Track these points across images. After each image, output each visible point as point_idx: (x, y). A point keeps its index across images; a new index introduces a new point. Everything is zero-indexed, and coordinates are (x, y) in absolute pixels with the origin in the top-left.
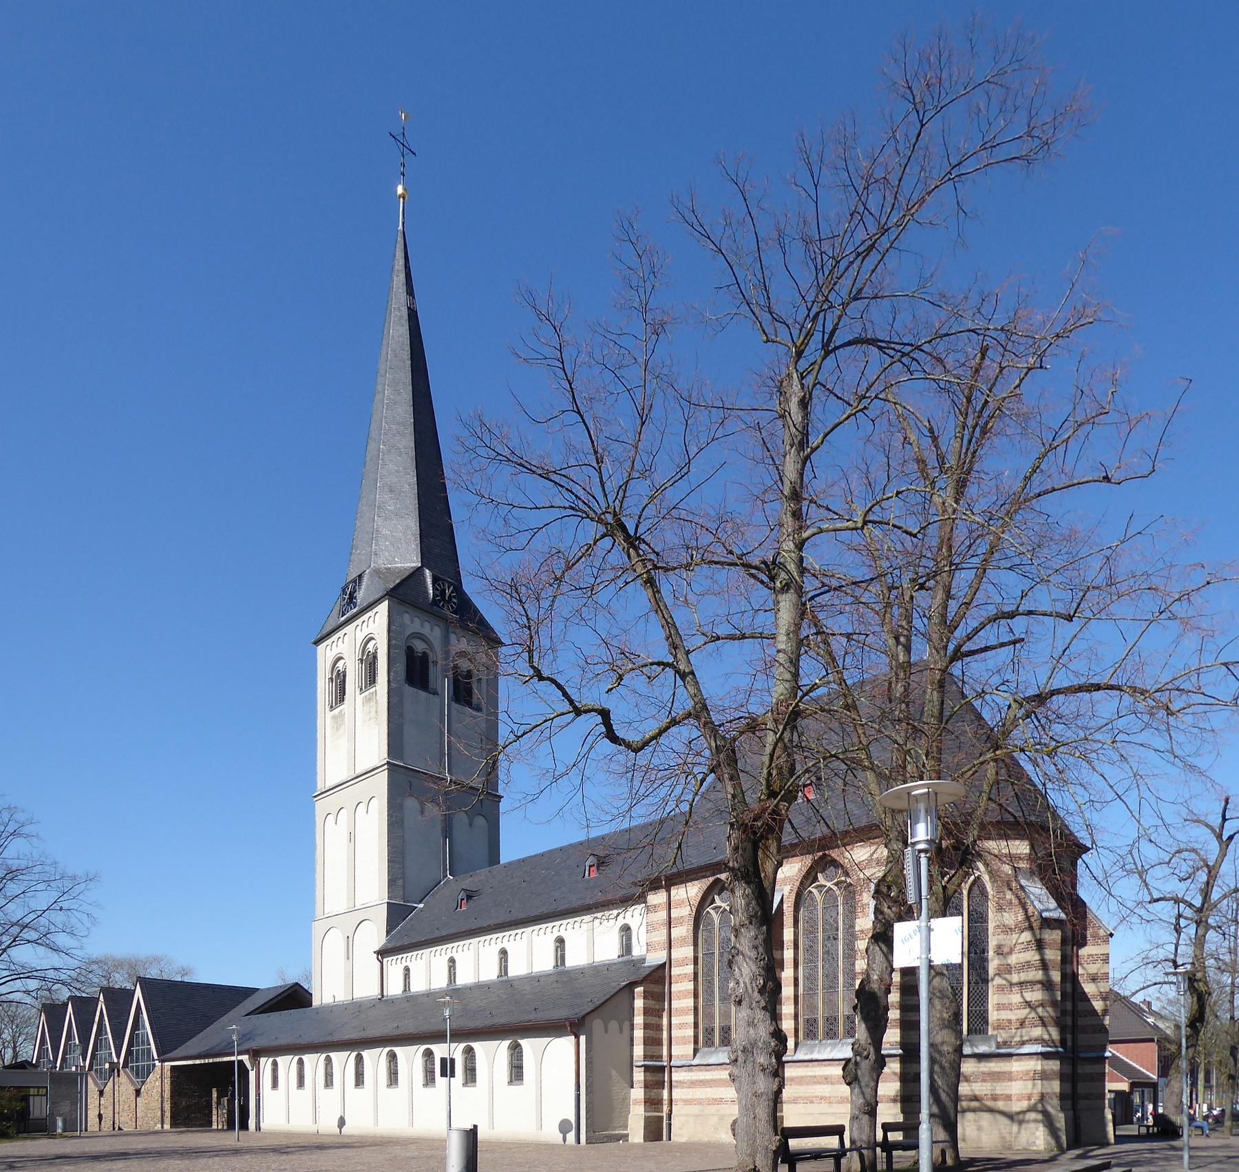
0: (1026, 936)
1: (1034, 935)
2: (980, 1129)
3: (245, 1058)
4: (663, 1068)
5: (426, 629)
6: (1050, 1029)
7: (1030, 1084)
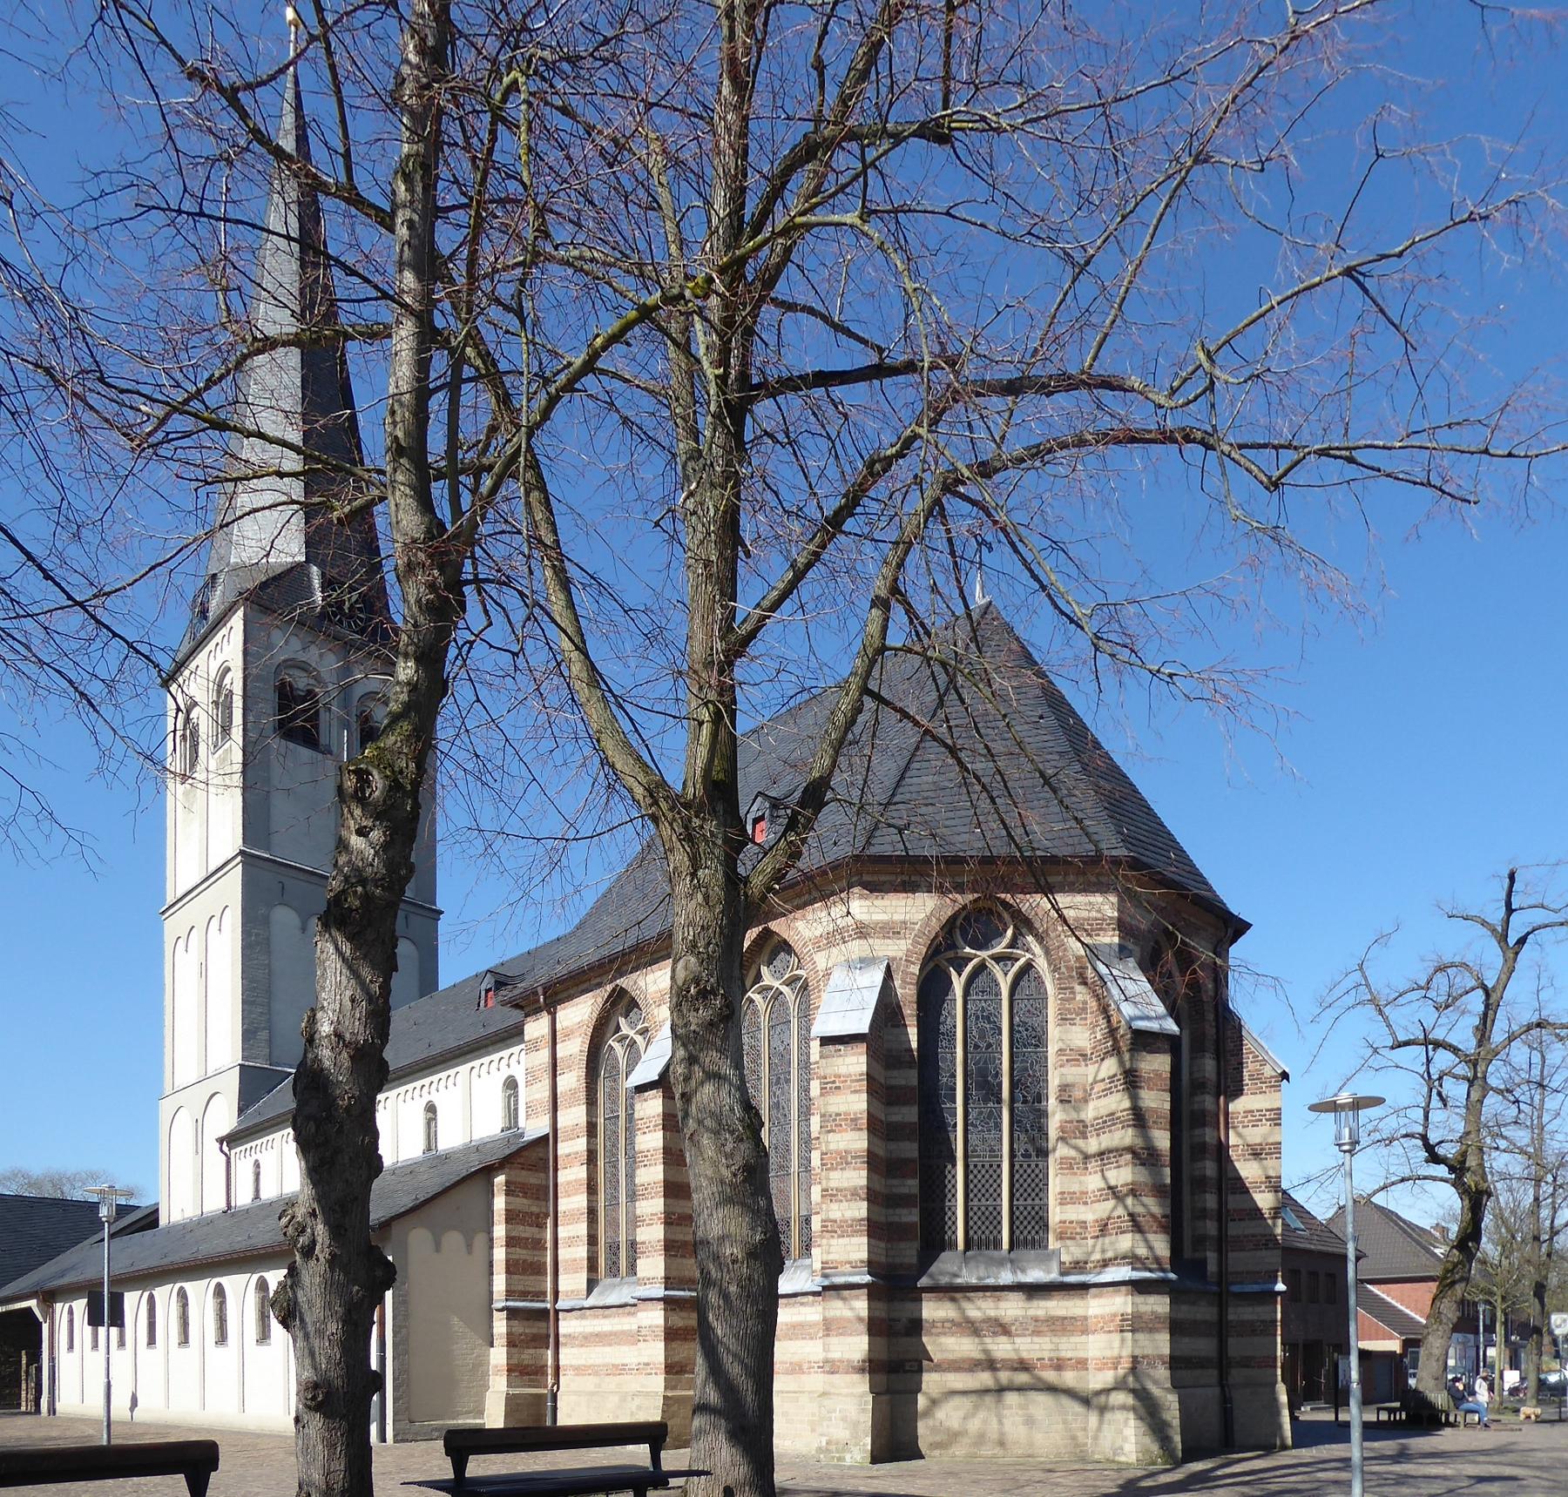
0: (1110, 1066)
1: (1121, 1063)
2: (1030, 1421)
3: (32, 1303)
4: (546, 1311)
5: (312, 655)
6: (1151, 1237)
7: (1116, 1337)
